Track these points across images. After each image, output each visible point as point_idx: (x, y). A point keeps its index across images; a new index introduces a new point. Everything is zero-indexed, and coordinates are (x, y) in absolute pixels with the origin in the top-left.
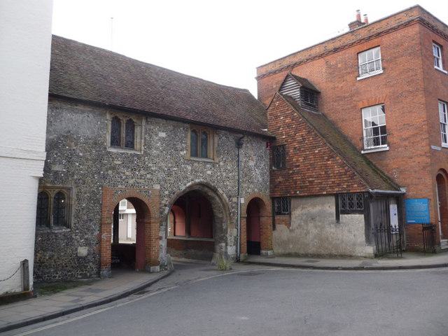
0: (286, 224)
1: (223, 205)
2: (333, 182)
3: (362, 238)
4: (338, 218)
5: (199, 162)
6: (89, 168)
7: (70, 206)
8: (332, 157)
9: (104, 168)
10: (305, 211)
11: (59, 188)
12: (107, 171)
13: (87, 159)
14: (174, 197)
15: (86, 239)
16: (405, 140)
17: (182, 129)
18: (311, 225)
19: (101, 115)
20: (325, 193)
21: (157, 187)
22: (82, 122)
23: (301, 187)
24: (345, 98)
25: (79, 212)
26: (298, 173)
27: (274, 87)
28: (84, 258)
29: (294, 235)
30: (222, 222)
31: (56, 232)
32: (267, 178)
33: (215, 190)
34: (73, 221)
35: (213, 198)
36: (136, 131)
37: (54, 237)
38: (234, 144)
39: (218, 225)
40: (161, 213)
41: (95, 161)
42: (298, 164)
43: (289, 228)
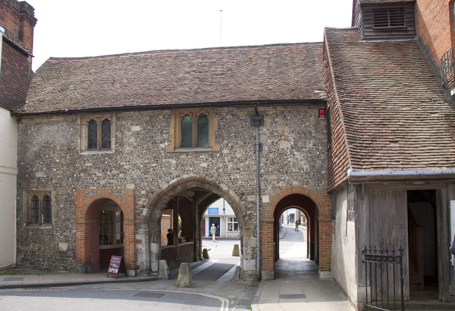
5: (187, 154)
6: (64, 172)
9: (77, 172)
11: (35, 192)
12: (79, 174)
13: (62, 165)
15: (66, 236)
17: (161, 117)
21: (132, 186)
22: (58, 131)
25: (58, 212)
28: (65, 253)
31: (42, 228)
37: (40, 232)
41: (68, 165)
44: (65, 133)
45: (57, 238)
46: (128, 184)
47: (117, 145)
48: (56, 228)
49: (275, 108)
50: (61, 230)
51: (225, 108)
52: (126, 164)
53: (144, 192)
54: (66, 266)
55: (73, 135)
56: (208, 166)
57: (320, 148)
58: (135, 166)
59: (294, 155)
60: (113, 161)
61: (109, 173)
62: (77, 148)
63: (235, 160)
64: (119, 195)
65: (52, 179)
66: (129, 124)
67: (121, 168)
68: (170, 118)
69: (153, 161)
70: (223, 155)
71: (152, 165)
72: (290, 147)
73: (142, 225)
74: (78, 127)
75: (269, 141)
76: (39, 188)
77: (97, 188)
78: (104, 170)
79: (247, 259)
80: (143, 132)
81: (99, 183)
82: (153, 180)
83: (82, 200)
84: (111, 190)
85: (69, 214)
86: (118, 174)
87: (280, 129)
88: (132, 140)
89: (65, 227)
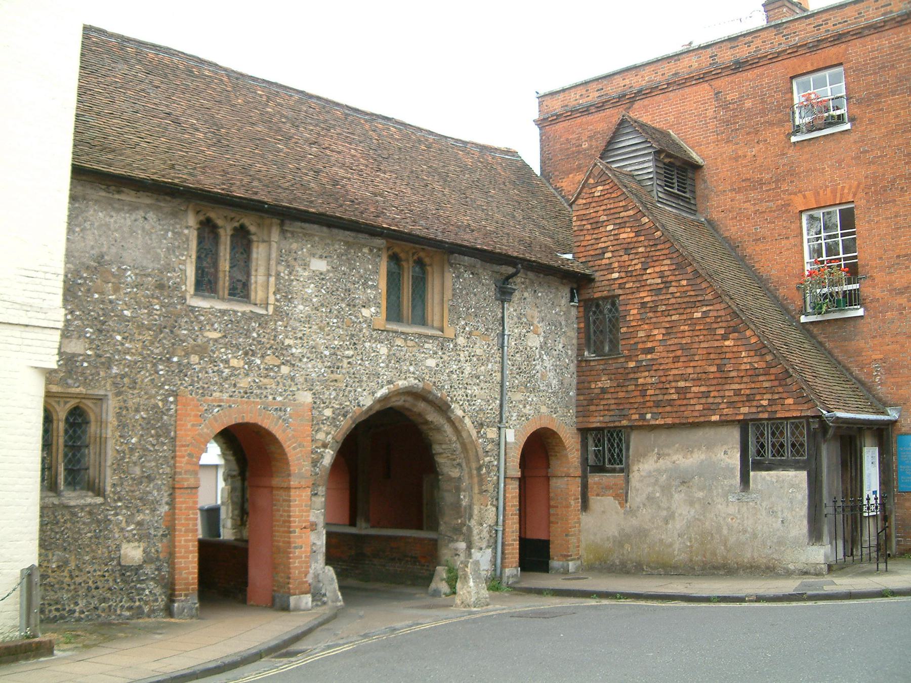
0: (616, 496)
1: (464, 445)
2: (737, 393)
3: (800, 527)
4: (745, 479)
6: (144, 347)
7: (102, 441)
8: (735, 330)
10: (663, 463)
12: (187, 355)
13: (141, 326)
14: (346, 424)
15: (139, 524)
16: (901, 293)
17: (366, 250)
18: (678, 497)
19: (174, 214)
20: (715, 418)
21: (306, 398)
22: (132, 231)
23: (657, 404)
24: (761, 183)
25: (124, 458)
26: (648, 368)
27: (585, 146)
28: (137, 569)
29: (634, 522)
30: (458, 489)
31: (72, 503)
32: (570, 378)
33: (443, 408)
34: (110, 479)
35: (438, 429)
36: (254, 255)
37: (67, 517)
38: (491, 292)
39: (448, 498)
40: (315, 463)
42: (649, 345)
43: (622, 506)
44: (151, 239)
45: (116, 530)
46: (300, 392)
47: (278, 296)
48: (115, 501)
49: (526, 275)
50: (127, 507)
51: (466, 258)
52: (296, 346)
53: (328, 413)
54: (140, 607)
55: (174, 251)
56: (437, 365)
57: (570, 352)
58: (314, 350)
59: (543, 360)
60: (268, 334)
61: (258, 361)
62: (183, 287)
63: (475, 359)
64: (280, 417)
65: (108, 365)
66: (305, 250)
67: (284, 352)
68: (379, 256)
69: (348, 343)
70: (458, 348)
71: (347, 352)
72: (538, 346)
73: (320, 488)
74: (186, 231)
75: (516, 331)
76: (69, 386)
77: (231, 396)
78: (246, 354)
79: (481, 549)
80: (331, 275)
81: (235, 385)
82: (346, 386)
83: (193, 425)
84: (262, 403)
85: (153, 464)
86: (278, 366)
87: (529, 311)
88: (310, 291)
89: (141, 499)
